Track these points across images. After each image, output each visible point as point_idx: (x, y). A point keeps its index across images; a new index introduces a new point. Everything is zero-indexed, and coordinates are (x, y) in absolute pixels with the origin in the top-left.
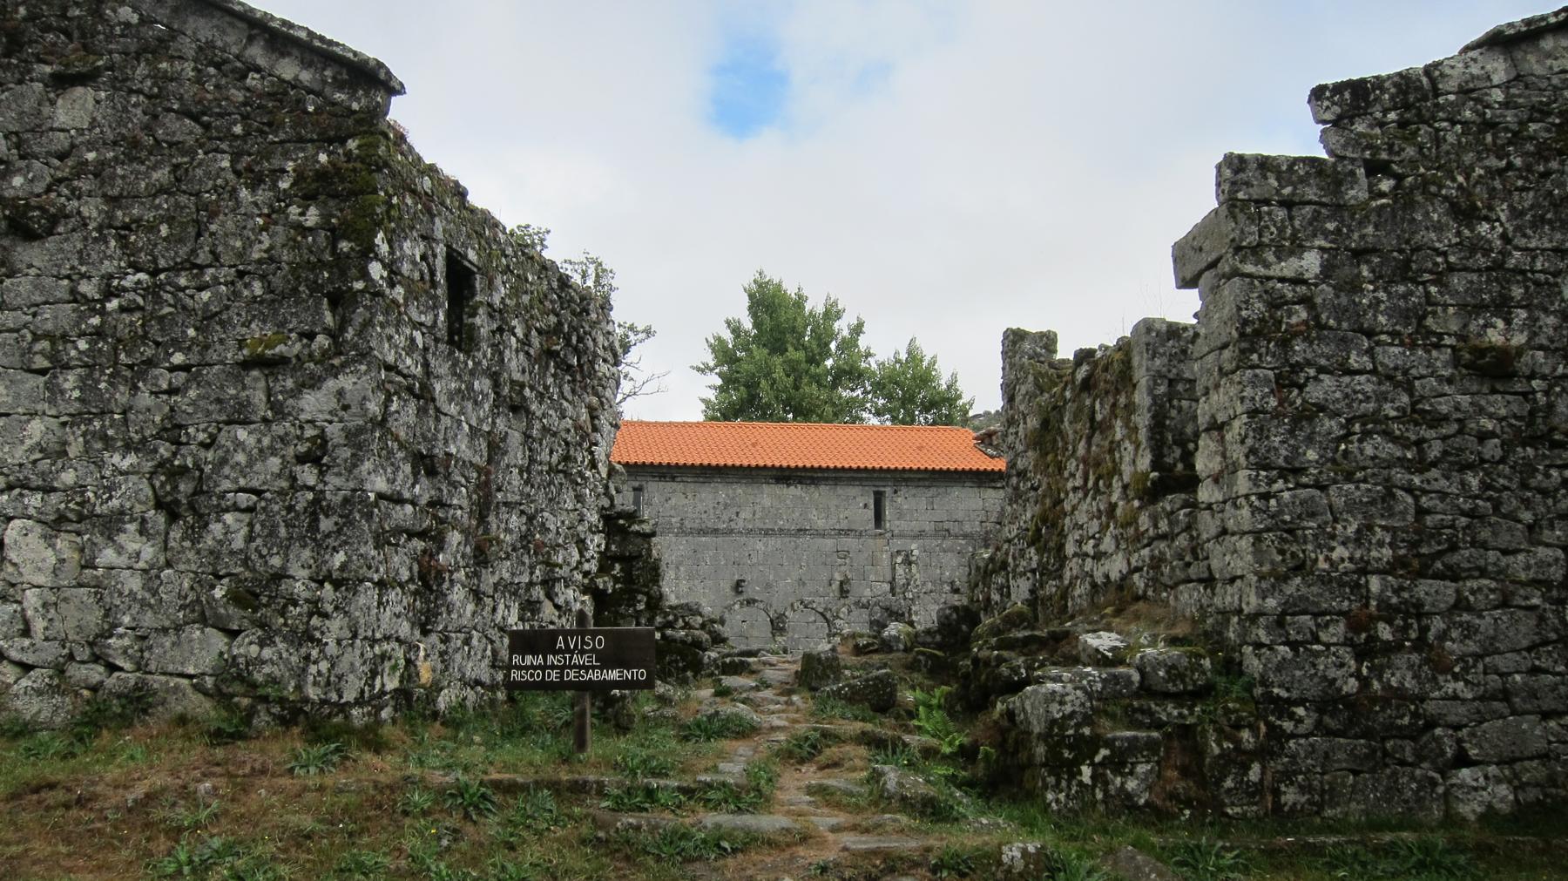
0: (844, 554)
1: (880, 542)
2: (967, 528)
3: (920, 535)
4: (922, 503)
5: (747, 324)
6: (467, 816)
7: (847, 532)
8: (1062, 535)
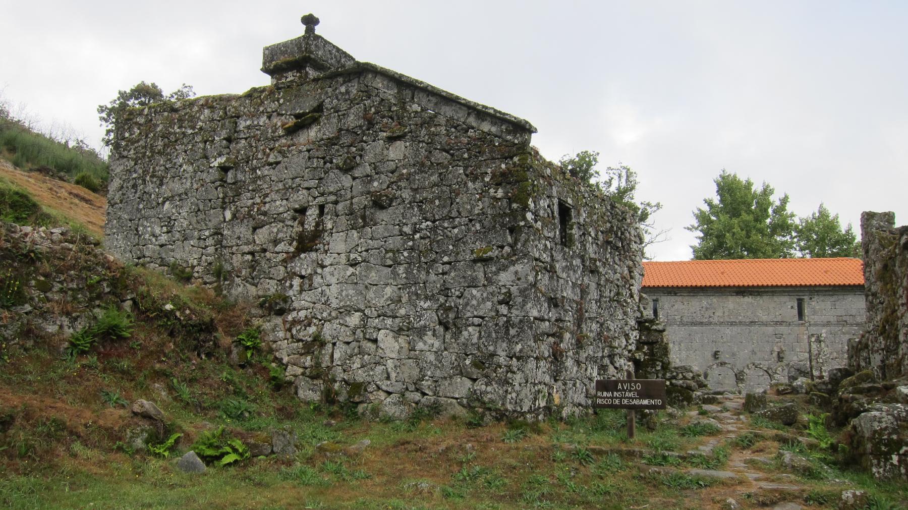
0: (779, 336)
2: (859, 319)
3: (828, 324)
5: (716, 200)
6: (581, 463)
7: (781, 323)
8: (897, 330)
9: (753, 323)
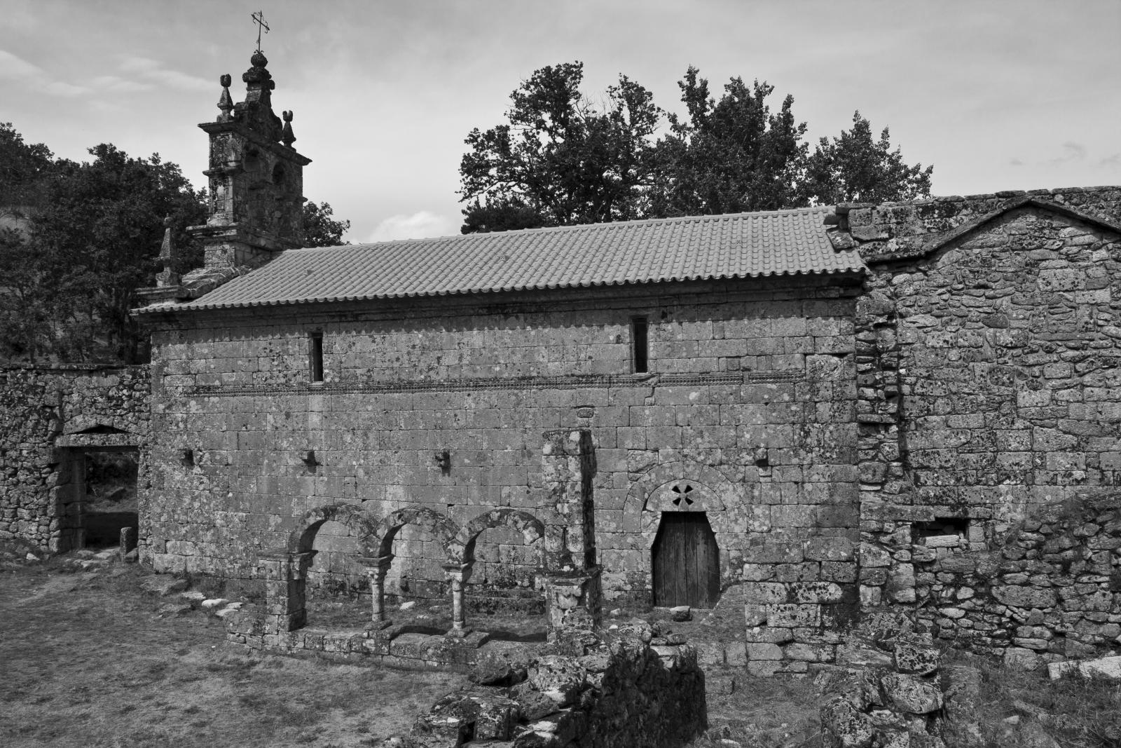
1: (641, 390)
2: (781, 365)
4: (706, 329)
7: (589, 379)
9: (525, 381)
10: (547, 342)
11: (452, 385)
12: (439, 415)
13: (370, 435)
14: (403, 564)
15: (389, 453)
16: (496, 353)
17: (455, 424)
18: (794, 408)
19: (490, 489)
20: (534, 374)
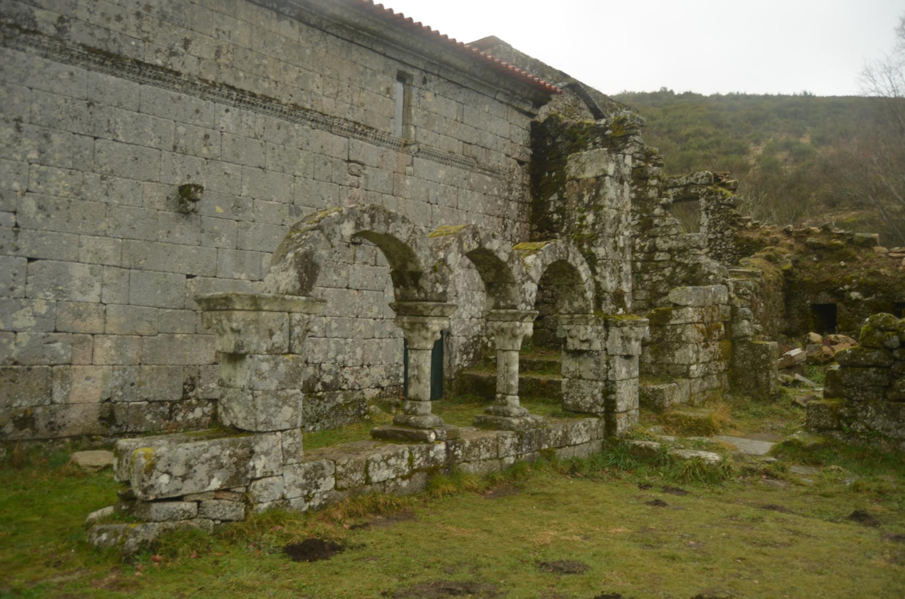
1: (405, 158)
10: (323, 70)
11: (208, 88)
12: (181, 130)
13: (57, 139)
14: (105, 378)
15: (91, 178)
16: (265, 62)
17: (205, 151)
18: (499, 202)
19: (248, 254)
20: (308, 106)
